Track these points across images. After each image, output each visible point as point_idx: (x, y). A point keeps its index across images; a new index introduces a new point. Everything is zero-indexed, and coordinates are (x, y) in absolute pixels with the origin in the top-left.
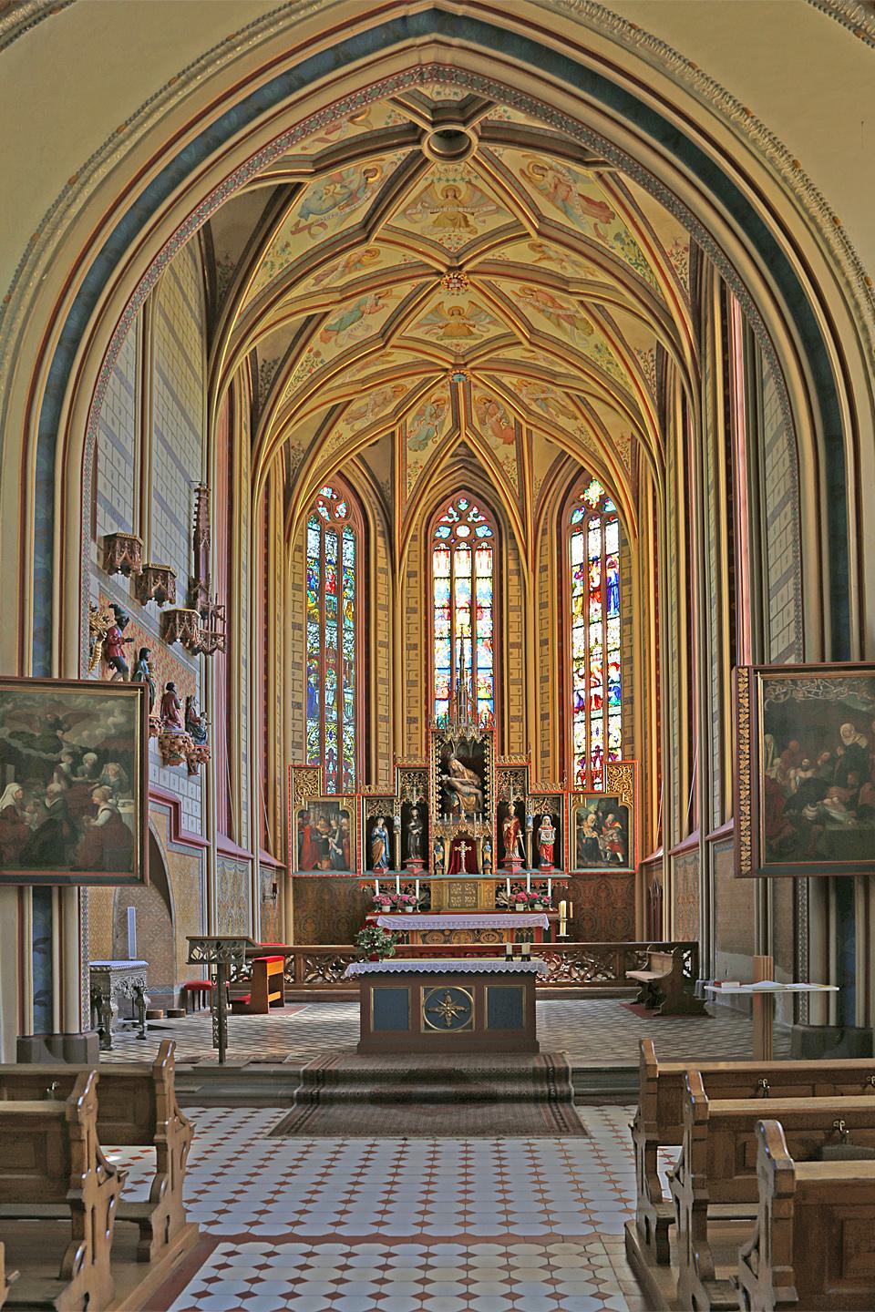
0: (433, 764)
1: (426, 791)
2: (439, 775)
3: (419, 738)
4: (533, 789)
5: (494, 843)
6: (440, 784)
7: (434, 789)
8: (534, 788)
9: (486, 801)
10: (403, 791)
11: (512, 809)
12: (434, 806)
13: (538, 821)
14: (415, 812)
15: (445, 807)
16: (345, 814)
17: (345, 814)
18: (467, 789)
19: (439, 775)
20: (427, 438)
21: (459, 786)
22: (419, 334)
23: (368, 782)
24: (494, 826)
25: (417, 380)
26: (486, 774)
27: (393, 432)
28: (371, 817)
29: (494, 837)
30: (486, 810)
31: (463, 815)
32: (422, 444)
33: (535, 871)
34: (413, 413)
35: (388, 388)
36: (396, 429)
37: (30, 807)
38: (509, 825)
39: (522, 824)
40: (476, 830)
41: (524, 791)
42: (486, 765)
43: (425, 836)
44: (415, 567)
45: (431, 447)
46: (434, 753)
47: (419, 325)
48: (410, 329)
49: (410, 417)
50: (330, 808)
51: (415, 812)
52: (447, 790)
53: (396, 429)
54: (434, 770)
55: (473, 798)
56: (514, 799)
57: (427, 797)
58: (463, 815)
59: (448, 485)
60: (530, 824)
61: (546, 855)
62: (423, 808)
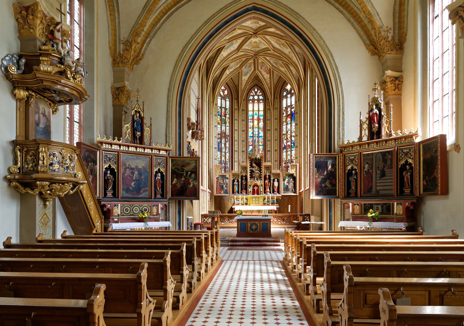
0: (249, 164)
1: (247, 172)
2: (250, 168)
3: (244, 157)
4: (273, 171)
5: (263, 186)
6: (250, 170)
7: (249, 171)
8: (273, 171)
9: (261, 175)
10: (241, 172)
11: (268, 177)
12: (249, 176)
13: (274, 181)
14: (244, 178)
15: (252, 177)
16: (227, 178)
17: (227, 178)
18: (257, 172)
19: (250, 168)
20: (247, 73)
21: (255, 171)
22: (246, 48)
23: (232, 170)
24: (263, 182)
25: (245, 58)
26: (261, 167)
27: (239, 72)
28: (234, 179)
29: (263, 185)
30: (261, 177)
31: (256, 179)
32: (246, 74)
33: (273, 194)
34: (244, 66)
35: (238, 61)
36: (240, 71)
37: (178, 184)
38: (267, 181)
39: (270, 181)
40: (259, 183)
41: (270, 172)
42: (261, 165)
43: (246, 184)
44: (244, 108)
45: (248, 75)
46: (248, 162)
47: (246, 46)
48: (245, 47)
49: (243, 68)
50: (223, 177)
51: (244, 178)
52: (252, 172)
53: (240, 71)
54: (249, 166)
55: (258, 174)
56: (268, 174)
57: (247, 173)
58: (256, 179)
59: (252, 84)
60: (272, 181)
61: (276, 190)
62: (246, 177)
